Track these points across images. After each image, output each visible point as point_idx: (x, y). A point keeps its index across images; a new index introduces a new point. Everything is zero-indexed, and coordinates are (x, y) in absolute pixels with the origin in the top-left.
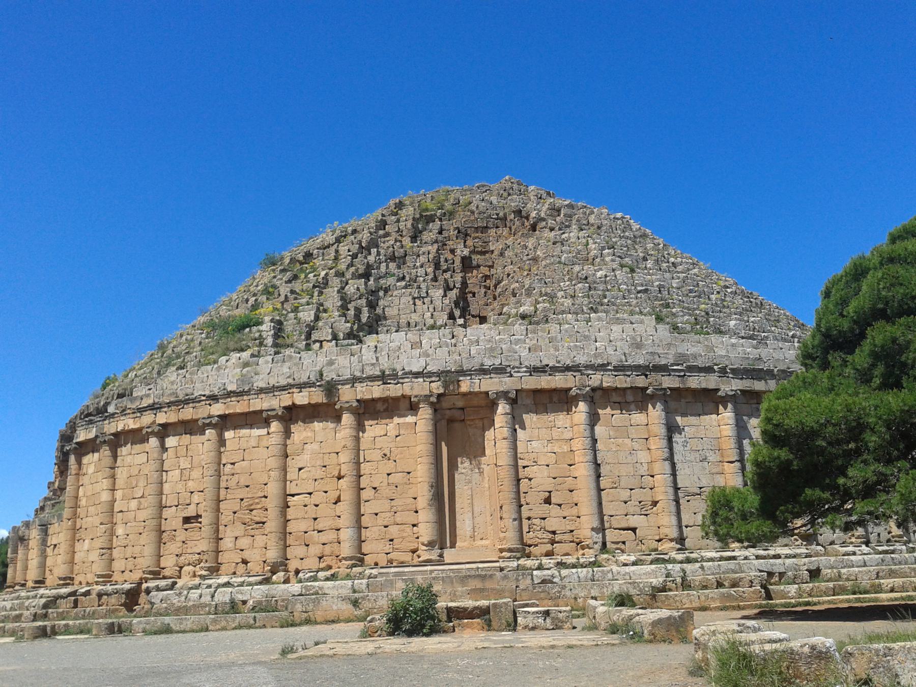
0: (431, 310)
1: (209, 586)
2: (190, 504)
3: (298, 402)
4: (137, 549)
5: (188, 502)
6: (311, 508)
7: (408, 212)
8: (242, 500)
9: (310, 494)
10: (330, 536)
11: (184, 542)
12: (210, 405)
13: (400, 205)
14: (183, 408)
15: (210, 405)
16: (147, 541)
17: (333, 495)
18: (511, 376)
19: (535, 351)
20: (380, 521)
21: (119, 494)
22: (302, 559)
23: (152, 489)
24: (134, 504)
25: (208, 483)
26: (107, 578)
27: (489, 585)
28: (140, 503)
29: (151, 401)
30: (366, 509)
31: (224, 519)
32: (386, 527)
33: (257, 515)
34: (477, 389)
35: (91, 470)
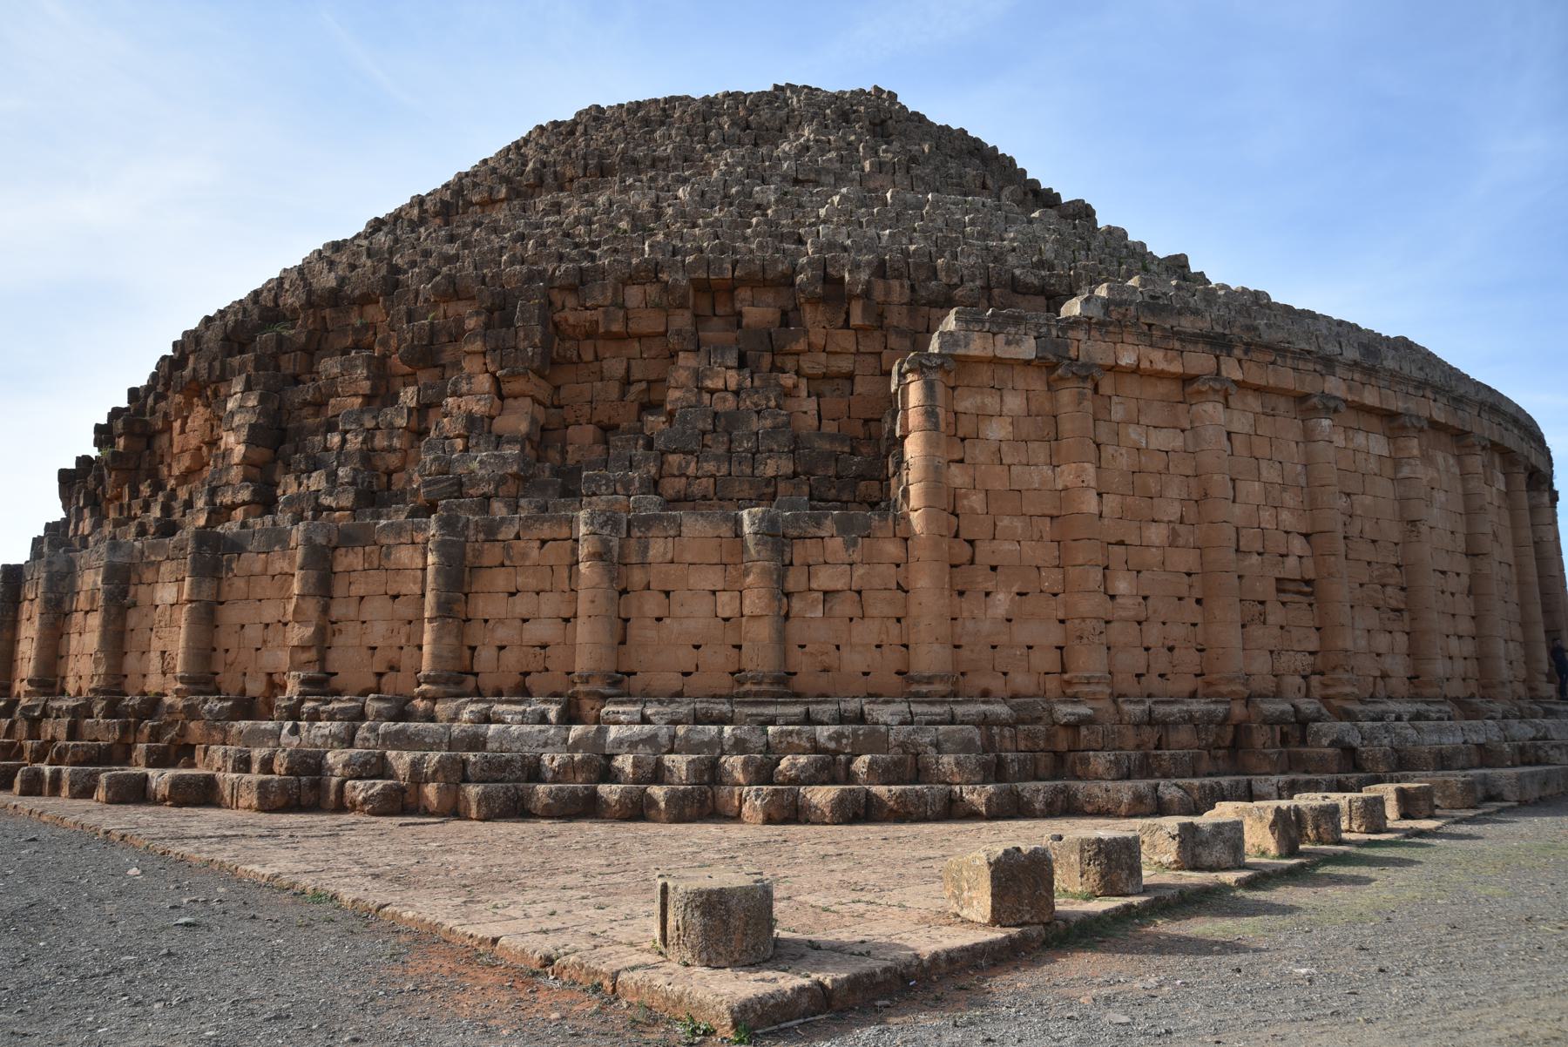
2: (1287, 555)
5: (1283, 551)
11: (1282, 627)
14: (1273, 363)
21: (1111, 502)
24: (1157, 534)
28: (1174, 534)
29: (1203, 325)
33: (1394, 597)
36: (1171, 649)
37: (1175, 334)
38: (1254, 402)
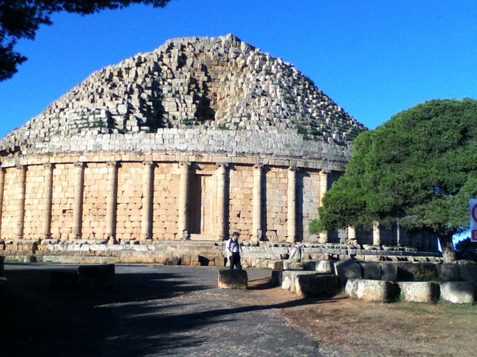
0: (186, 111)
1: (77, 244)
3: (123, 160)
4: (37, 224)
6: (128, 210)
7: (175, 52)
8: (94, 204)
9: (128, 204)
10: (137, 224)
12: (79, 156)
13: (171, 46)
14: (65, 156)
15: (79, 156)
16: (44, 220)
17: (139, 205)
18: (227, 156)
19: (239, 144)
20: (162, 219)
21: (27, 196)
22: (122, 234)
23: (46, 195)
24: (36, 201)
25: (77, 195)
26: (22, 235)
27: (209, 251)
28: (39, 201)
29: (47, 151)
30: (155, 213)
31: (84, 212)
32: (163, 222)
33: (101, 212)
34: (210, 161)
35: (11, 182)
36: (37, 227)
37: (39, 154)
38: (62, 166)
